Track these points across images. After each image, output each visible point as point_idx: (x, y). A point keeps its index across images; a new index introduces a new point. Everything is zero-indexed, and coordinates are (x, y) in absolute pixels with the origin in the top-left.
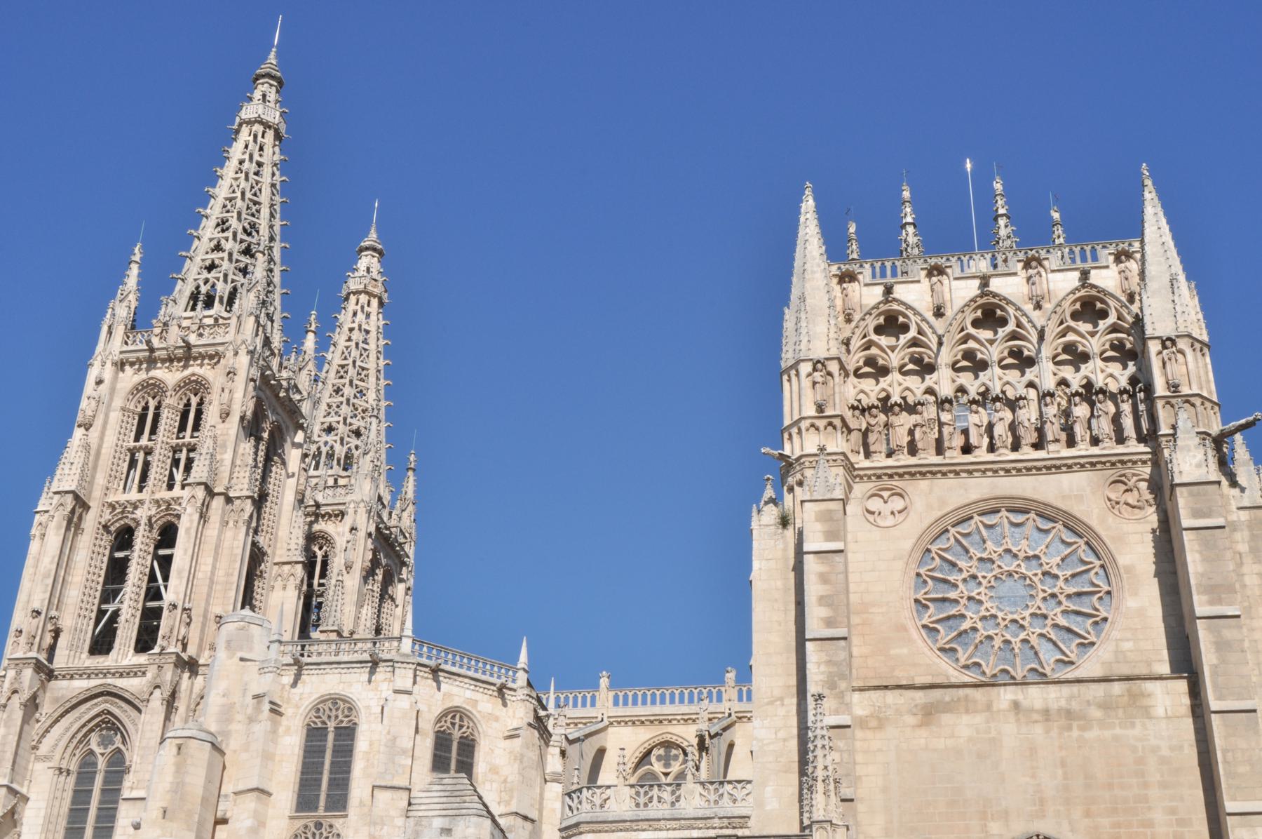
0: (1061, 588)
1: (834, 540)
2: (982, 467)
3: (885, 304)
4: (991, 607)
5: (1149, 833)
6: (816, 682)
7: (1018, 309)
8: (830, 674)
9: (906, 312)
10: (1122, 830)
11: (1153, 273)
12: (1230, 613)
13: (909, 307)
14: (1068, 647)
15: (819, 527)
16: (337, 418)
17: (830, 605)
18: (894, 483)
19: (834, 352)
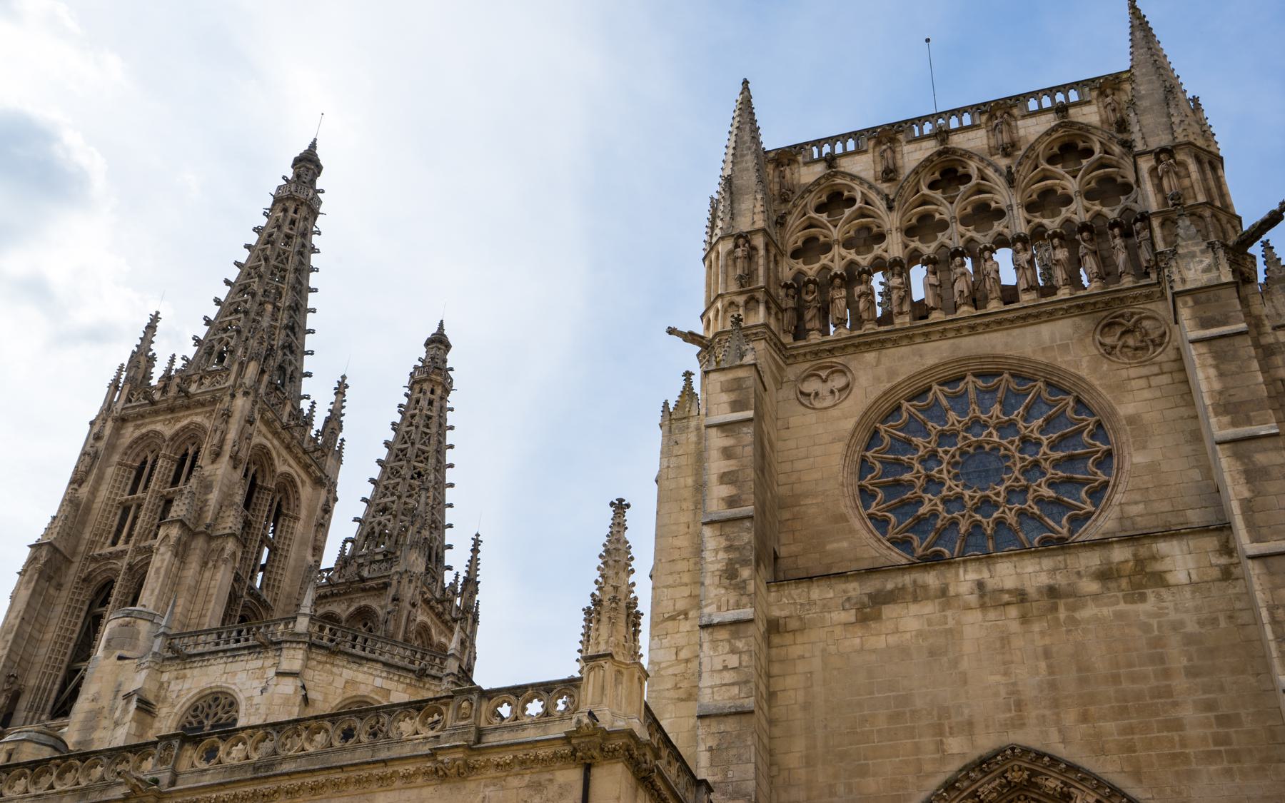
0: (1045, 453)
1: (742, 410)
2: (940, 328)
3: (828, 179)
4: (957, 486)
5: (1177, 739)
6: (713, 572)
7: (982, 160)
8: (730, 563)
9: (851, 184)
10: (1136, 737)
11: (1143, 92)
12: (1263, 433)
13: (853, 177)
14: (1059, 523)
15: (725, 397)
16: (391, 499)
17: (732, 483)
18: (834, 360)
19: (760, 224)
